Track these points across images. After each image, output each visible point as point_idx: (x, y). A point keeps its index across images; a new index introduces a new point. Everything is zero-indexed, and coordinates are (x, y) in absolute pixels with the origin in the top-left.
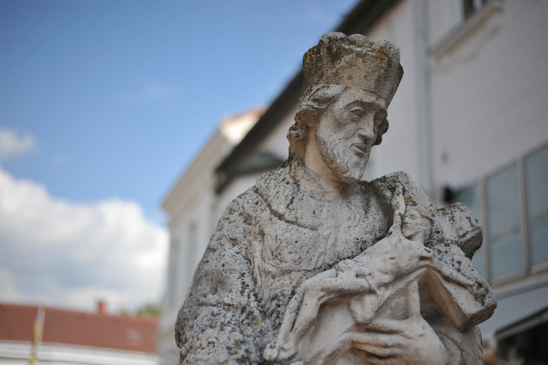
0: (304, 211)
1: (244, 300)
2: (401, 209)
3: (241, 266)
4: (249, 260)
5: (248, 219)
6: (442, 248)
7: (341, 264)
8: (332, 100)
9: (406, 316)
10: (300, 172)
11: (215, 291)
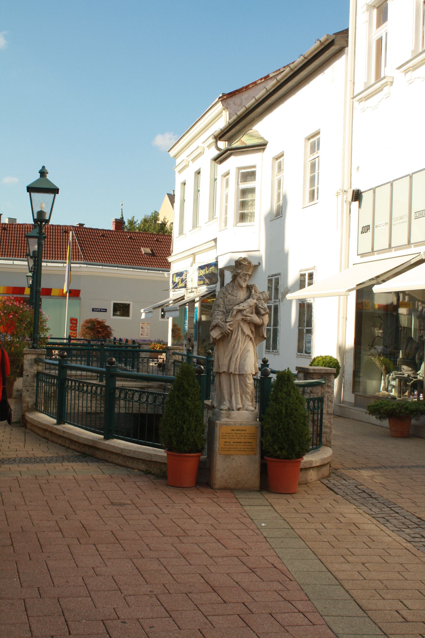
0: (234, 293)
1: (223, 310)
2: (253, 293)
3: (222, 303)
4: (224, 302)
5: (224, 294)
6: (260, 301)
7: (240, 304)
8: (239, 273)
9: (252, 313)
10: (234, 285)
11: (218, 308)
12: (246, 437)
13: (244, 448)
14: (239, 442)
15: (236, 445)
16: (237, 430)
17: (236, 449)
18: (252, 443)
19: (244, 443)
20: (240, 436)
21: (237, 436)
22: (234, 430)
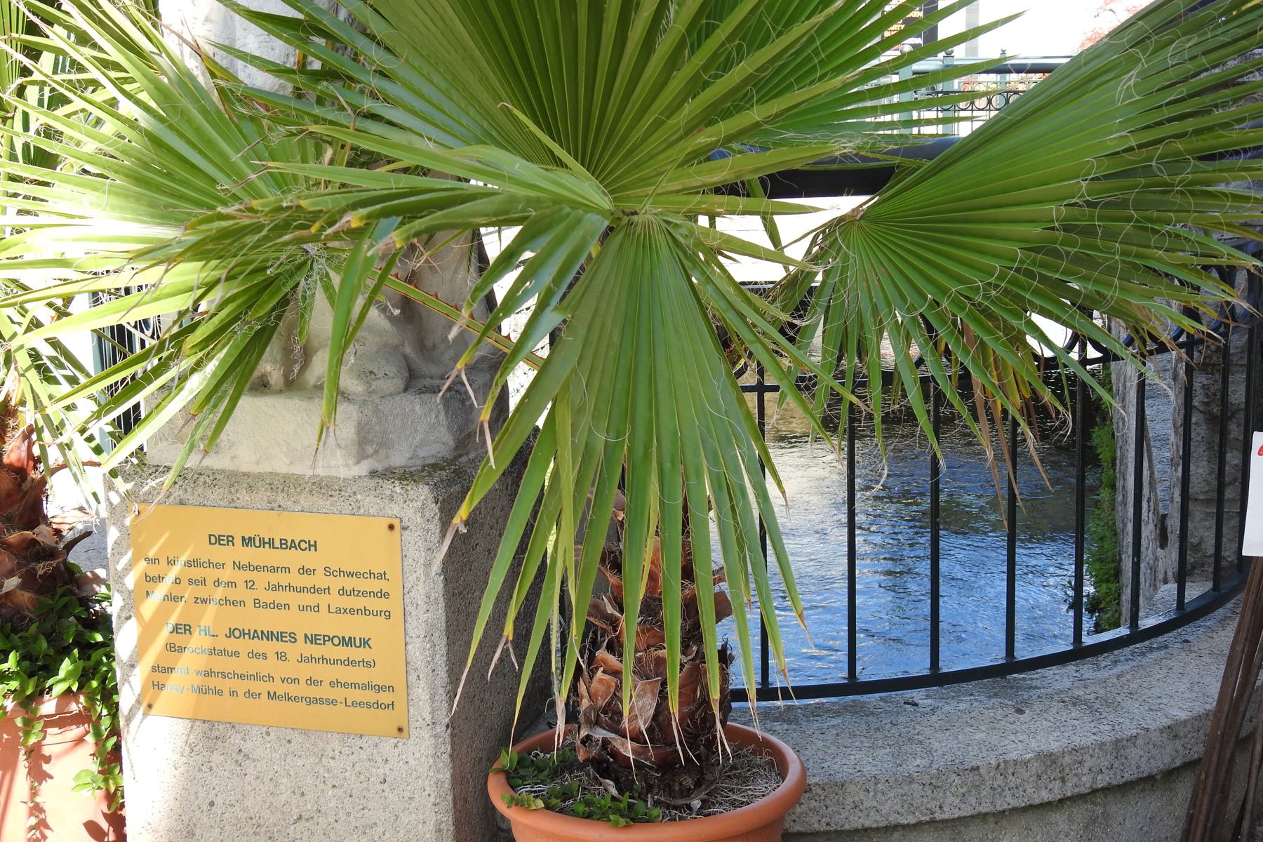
12: (323, 600)
13: (311, 682)
14: (269, 636)
15: (252, 655)
16: (247, 542)
17: (256, 686)
18: (365, 643)
19: (312, 639)
20: (278, 587)
21: (250, 585)
22: (230, 540)
